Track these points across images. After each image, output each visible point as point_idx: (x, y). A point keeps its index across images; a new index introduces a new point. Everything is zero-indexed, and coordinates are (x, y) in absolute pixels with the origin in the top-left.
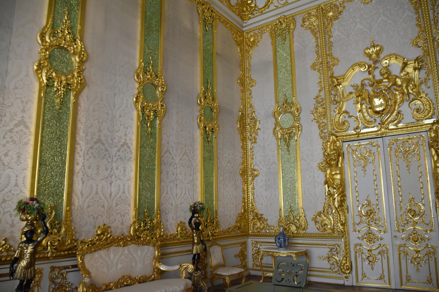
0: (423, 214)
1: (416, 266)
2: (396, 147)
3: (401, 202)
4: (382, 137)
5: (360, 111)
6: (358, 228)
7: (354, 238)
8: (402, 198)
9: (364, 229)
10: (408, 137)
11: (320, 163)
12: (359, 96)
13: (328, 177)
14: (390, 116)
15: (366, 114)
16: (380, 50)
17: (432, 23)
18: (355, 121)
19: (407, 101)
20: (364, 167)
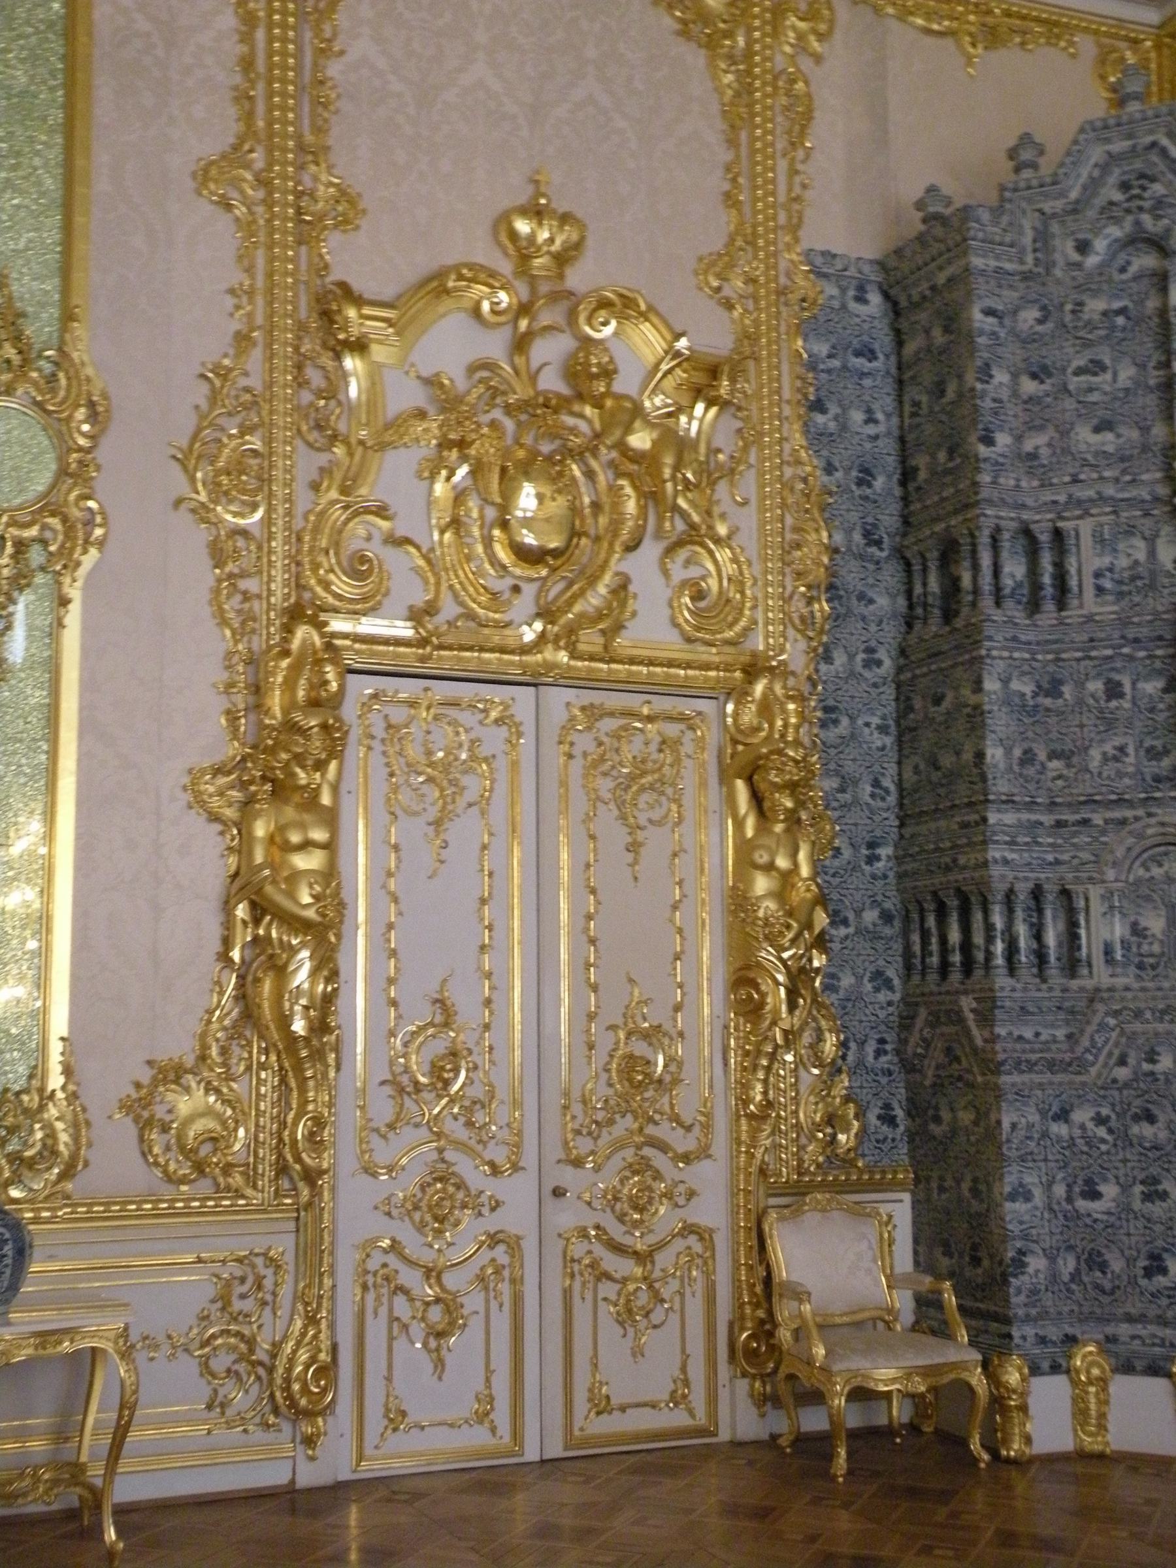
0: (676, 1081)
1: (631, 1331)
2: (591, 747)
3: (591, 1017)
4: (535, 685)
5: (456, 523)
6: (382, 1153)
7: (358, 1212)
8: (597, 1000)
9: (412, 1154)
10: (645, 711)
11: (203, 772)
12: (462, 444)
13: (259, 858)
14: (582, 593)
15: (480, 549)
16: (578, 246)
17: (782, 218)
18: (416, 570)
19: (659, 534)
20: (437, 823)
